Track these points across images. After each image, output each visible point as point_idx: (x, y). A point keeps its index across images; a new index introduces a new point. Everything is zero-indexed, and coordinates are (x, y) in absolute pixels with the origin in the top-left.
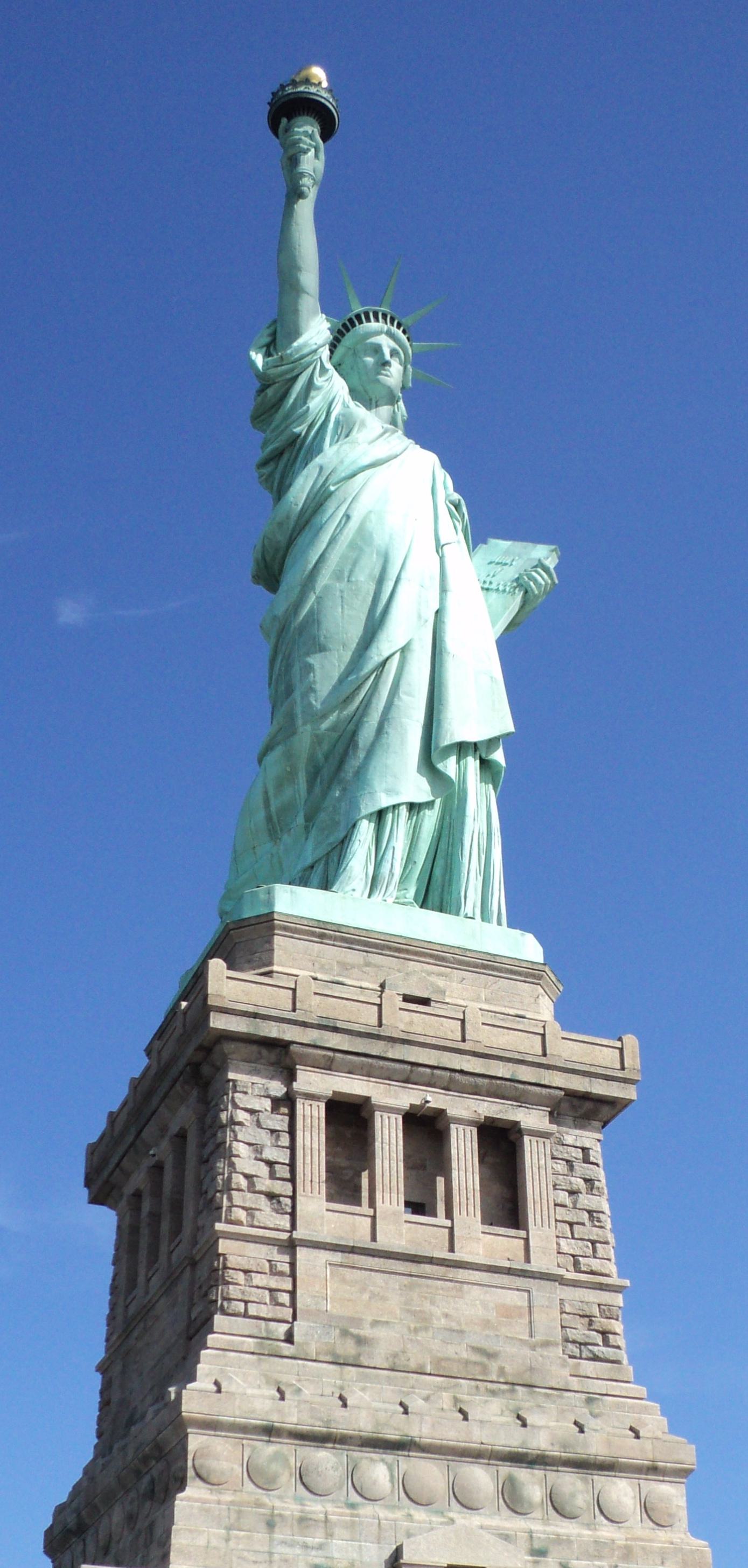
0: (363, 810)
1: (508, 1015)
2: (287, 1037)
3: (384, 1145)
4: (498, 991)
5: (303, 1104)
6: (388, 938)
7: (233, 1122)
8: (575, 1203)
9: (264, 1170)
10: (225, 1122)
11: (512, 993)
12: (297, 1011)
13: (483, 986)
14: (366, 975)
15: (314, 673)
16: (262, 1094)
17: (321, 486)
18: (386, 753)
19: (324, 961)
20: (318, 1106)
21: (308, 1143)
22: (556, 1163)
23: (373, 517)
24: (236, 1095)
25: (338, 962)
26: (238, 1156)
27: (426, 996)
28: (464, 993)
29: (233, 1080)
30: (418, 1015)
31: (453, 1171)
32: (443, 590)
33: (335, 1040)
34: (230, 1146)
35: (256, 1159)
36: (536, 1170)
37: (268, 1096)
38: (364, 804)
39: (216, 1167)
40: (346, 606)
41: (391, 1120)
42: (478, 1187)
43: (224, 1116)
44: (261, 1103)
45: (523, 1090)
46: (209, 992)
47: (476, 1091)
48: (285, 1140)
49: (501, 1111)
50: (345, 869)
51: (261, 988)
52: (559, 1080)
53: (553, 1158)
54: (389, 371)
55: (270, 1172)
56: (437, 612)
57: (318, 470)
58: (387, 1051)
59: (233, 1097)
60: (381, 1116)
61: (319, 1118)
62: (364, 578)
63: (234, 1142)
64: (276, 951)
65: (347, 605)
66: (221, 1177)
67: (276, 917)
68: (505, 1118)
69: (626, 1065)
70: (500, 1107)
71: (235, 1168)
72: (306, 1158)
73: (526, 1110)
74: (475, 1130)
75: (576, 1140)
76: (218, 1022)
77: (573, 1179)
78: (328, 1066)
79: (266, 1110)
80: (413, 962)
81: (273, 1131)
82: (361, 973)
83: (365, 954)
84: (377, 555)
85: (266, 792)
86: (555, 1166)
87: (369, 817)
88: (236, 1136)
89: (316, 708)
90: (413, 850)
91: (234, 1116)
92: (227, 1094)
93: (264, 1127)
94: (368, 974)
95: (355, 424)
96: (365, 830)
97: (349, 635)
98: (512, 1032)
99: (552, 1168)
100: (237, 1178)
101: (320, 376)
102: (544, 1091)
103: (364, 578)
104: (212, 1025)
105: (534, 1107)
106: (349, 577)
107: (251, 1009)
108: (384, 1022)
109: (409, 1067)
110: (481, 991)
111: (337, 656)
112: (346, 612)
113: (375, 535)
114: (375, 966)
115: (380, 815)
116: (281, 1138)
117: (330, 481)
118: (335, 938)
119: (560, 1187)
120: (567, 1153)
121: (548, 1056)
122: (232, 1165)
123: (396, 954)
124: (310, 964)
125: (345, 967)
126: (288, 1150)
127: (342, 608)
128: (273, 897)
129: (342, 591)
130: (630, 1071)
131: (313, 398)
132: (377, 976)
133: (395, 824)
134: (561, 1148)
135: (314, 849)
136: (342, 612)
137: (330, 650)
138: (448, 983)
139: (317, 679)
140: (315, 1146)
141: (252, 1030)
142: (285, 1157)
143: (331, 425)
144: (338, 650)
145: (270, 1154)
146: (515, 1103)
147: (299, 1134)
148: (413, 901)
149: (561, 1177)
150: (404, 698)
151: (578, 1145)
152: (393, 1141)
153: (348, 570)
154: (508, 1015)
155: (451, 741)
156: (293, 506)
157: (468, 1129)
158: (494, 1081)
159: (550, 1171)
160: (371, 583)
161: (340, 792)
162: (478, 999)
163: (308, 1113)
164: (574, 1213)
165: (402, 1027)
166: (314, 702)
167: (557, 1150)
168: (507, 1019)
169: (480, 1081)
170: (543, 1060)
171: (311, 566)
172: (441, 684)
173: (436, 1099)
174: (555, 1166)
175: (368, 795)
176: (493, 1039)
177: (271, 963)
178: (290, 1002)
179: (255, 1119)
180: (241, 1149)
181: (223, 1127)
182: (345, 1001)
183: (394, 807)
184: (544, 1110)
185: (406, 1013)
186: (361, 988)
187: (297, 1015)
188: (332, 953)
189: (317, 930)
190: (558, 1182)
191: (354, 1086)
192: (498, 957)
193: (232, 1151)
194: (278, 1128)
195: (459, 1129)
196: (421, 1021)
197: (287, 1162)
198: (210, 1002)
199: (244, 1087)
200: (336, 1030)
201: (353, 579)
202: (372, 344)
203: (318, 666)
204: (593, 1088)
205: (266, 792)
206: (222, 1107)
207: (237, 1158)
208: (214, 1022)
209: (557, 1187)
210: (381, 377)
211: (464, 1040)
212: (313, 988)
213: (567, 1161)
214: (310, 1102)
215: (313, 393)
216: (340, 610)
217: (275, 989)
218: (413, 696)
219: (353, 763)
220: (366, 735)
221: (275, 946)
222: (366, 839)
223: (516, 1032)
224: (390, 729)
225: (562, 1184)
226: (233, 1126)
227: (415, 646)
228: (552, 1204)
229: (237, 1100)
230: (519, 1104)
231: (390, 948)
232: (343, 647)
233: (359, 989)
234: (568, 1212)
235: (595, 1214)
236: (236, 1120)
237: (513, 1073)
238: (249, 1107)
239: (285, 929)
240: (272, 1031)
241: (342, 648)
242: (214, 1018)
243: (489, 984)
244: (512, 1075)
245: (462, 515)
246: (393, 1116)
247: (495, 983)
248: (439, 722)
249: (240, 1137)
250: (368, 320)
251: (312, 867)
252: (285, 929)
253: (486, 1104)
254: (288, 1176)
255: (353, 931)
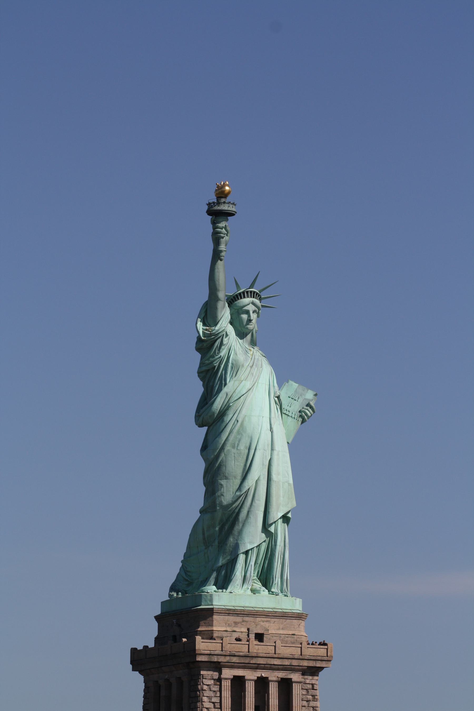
0: (241, 550)
1: (289, 635)
2: (220, 661)
3: (249, 693)
4: (286, 624)
5: (224, 681)
6: (250, 611)
7: (203, 690)
8: (309, 704)
9: (212, 705)
10: (200, 689)
11: (291, 625)
12: (223, 651)
13: (281, 623)
14: (243, 625)
15: (223, 488)
16: (211, 678)
17: (228, 402)
18: (250, 526)
19: (229, 622)
20: (229, 682)
21: (225, 696)
22: (303, 691)
23: (247, 419)
24: (204, 680)
25: (234, 622)
26: (204, 702)
27: (262, 632)
28: (275, 627)
29: (202, 674)
30: (261, 646)
31: (270, 699)
32: (272, 449)
33: (235, 660)
34: (202, 699)
35: (210, 702)
36: (296, 695)
37: (213, 679)
38: (241, 548)
39: (197, 705)
40: (236, 460)
41: (251, 683)
42: (277, 704)
43: (199, 687)
44: (211, 682)
45: (294, 668)
46: (196, 649)
47: (278, 669)
48: (218, 694)
49: (286, 675)
50: (235, 575)
51: (212, 644)
52: (306, 663)
53: (302, 689)
54: (252, 323)
55: (214, 705)
56: (270, 461)
57: (226, 395)
58: (250, 661)
59: (202, 680)
60: (248, 683)
61: (229, 686)
62: (243, 447)
63: (203, 697)
64: (214, 621)
65: (237, 460)
66: (199, 708)
67: (214, 609)
68: (287, 677)
69: (328, 655)
70: (286, 674)
71: (203, 706)
72: (225, 701)
73: (294, 674)
74: (277, 683)
75: (310, 681)
76: (199, 658)
77: (308, 696)
78: (232, 666)
79: (212, 684)
80: (258, 618)
81: (214, 691)
82: (241, 625)
83: (242, 617)
84: (248, 437)
85: (203, 529)
86: (302, 692)
87: (243, 553)
88: (203, 694)
89: (224, 504)
90: (257, 559)
91: (203, 688)
92: (201, 679)
93: (212, 690)
94: (243, 625)
95: (240, 366)
96: (242, 558)
97: (237, 473)
98: (291, 647)
99: (302, 693)
100: (204, 709)
101: (225, 338)
102: (300, 667)
103: (243, 447)
104: (197, 660)
105: (297, 672)
106: (237, 448)
107: (208, 652)
108: (250, 651)
109: (257, 665)
110: (280, 626)
111: (232, 482)
112: (236, 463)
113: (247, 428)
114: (246, 621)
115: (246, 553)
116: (217, 694)
117: (230, 401)
118: (233, 614)
119: (304, 700)
120: (307, 687)
121: (302, 656)
122: (202, 704)
123: (253, 616)
124: (225, 624)
125: (236, 623)
126: (219, 698)
127: (235, 462)
128: (213, 598)
129: (234, 454)
130: (330, 657)
131: (223, 349)
132: (246, 625)
133: (252, 554)
134: (305, 685)
135: (222, 561)
136: (235, 463)
137: (229, 479)
138: (269, 624)
139: (225, 491)
140: (228, 696)
141: (209, 660)
142: (218, 700)
143: (230, 365)
144: (233, 479)
145: (214, 700)
146: (291, 672)
147: (223, 692)
148: (256, 578)
149: (304, 696)
150: (256, 502)
151: (310, 683)
152: (251, 691)
153: (237, 443)
154: (289, 635)
155: (273, 521)
156: (216, 410)
157: (275, 683)
158: (284, 666)
159: (301, 694)
160: (245, 450)
161: (232, 539)
162: (279, 629)
163: (225, 684)
164: (308, 709)
165: (255, 651)
166: (223, 501)
167: (303, 686)
168: (289, 636)
169: (280, 667)
170: (301, 657)
171: (223, 442)
172: (269, 494)
173: (264, 674)
174: (302, 692)
175: (243, 544)
176: (284, 651)
177: (212, 625)
178: (221, 647)
179: (209, 687)
180: (205, 699)
181: (199, 691)
182: (237, 644)
183: (252, 549)
184: (300, 673)
185: (257, 646)
186: (241, 632)
187: (223, 653)
188: (232, 619)
189: (227, 612)
190: (303, 698)
191: (239, 672)
192: (287, 613)
193: (202, 700)
194: (216, 690)
195: (272, 684)
196: (261, 648)
197: (219, 702)
198: (197, 652)
199: (206, 677)
200: (235, 656)
201: (239, 448)
202: (245, 310)
203: (225, 486)
204: (317, 665)
205: (203, 529)
206: (199, 684)
207: (204, 703)
208: (197, 659)
209: (303, 700)
210: (248, 326)
211: (275, 653)
212: (228, 642)
213: (306, 689)
214: (226, 680)
215: (223, 347)
216: (234, 462)
217: (216, 643)
218: (260, 501)
219: (237, 528)
220: (242, 517)
221: (214, 619)
222: (241, 563)
223: (292, 647)
224: (251, 516)
225: (305, 698)
226: (202, 691)
227: (262, 478)
228: (301, 705)
229: (203, 682)
230: (292, 672)
231: (251, 615)
232: (235, 478)
233: (241, 633)
234: (306, 709)
235: (314, 708)
236: (204, 689)
237: (290, 663)
238: (207, 684)
239: (217, 613)
240: (215, 659)
241: (234, 478)
242: (198, 657)
243: (283, 622)
244: (290, 664)
245: (279, 400)
246: (251, 682)
247: (285, 621)
248: (269, 512)
249: (205, 695)
250: (244, 297)
251: (221, 566)
252: (217, 613)
253: (281, 673)
254: (219, 707)
255: (239, 611)
